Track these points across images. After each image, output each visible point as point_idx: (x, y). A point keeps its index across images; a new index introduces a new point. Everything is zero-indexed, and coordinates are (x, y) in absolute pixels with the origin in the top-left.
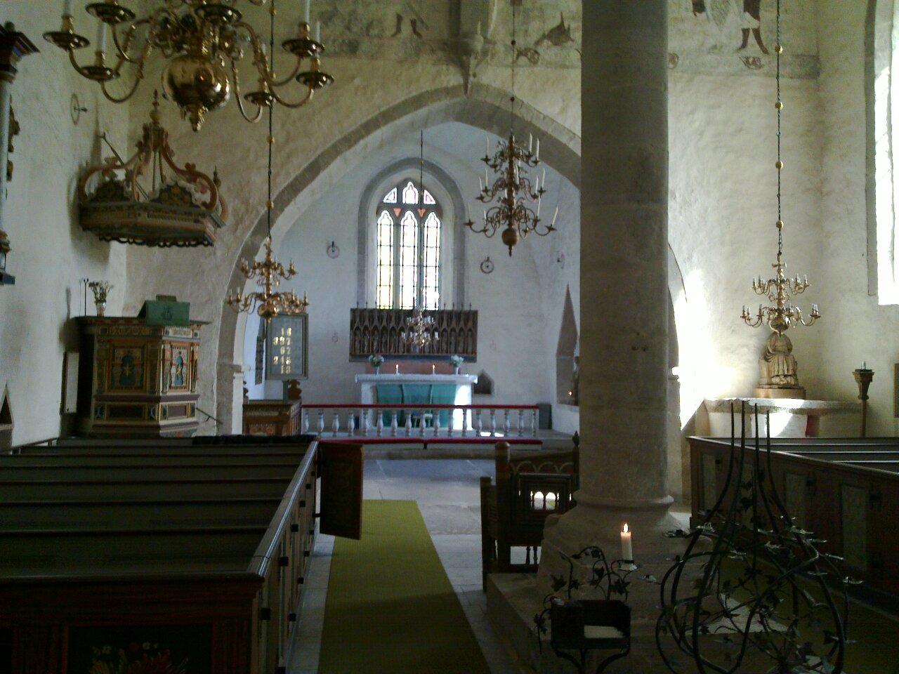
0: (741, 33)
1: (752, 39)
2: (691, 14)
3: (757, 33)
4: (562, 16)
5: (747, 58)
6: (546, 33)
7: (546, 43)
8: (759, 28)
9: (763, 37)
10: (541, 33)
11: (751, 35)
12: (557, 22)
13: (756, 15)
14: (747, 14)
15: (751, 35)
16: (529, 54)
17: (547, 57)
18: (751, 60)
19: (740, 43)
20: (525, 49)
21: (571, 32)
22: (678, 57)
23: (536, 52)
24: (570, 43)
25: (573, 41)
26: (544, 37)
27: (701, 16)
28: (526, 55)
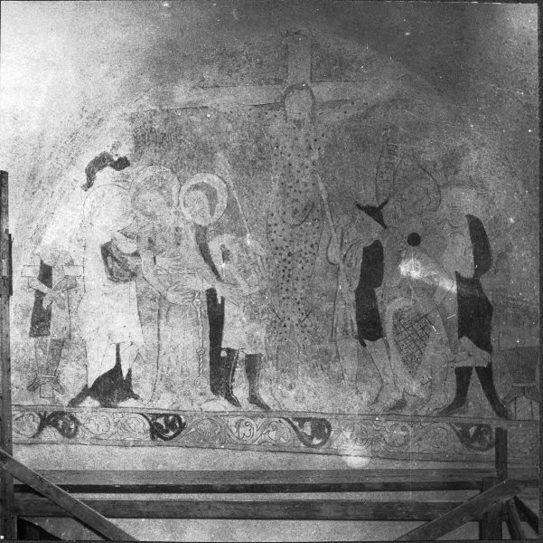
0: (452, 378)
1: (476, 391)
2: (354, 344)
3: (486, 374)
4: (118, 354)
5: (466, 427)
6: (90, 386)
7: (90, 403)
8: (490, 365)
9: (500, 384)
10: (81, 384)
11: (475, 378)
12: (111, 365)
13: (483, 343)
14: (465, 340)
15: (475, 378)
16: (61, 422)
17: (91, 426)
18: (472, 430)
19: (452, 395)
20: (54, 414)
21: (133, 382)
22: (329, 427)
23: (73, 419)
24: (130, 403)
25: (136, 397)
26: (86, 392)
27: (374, 347)
28: (55, 425)
